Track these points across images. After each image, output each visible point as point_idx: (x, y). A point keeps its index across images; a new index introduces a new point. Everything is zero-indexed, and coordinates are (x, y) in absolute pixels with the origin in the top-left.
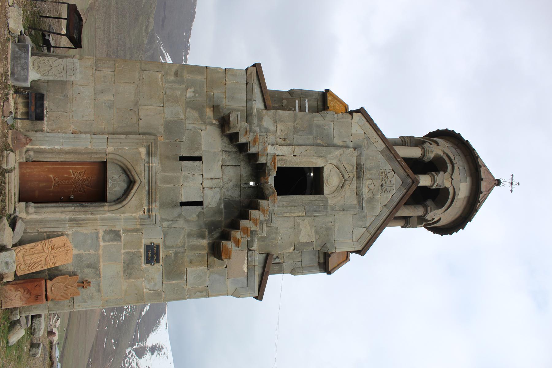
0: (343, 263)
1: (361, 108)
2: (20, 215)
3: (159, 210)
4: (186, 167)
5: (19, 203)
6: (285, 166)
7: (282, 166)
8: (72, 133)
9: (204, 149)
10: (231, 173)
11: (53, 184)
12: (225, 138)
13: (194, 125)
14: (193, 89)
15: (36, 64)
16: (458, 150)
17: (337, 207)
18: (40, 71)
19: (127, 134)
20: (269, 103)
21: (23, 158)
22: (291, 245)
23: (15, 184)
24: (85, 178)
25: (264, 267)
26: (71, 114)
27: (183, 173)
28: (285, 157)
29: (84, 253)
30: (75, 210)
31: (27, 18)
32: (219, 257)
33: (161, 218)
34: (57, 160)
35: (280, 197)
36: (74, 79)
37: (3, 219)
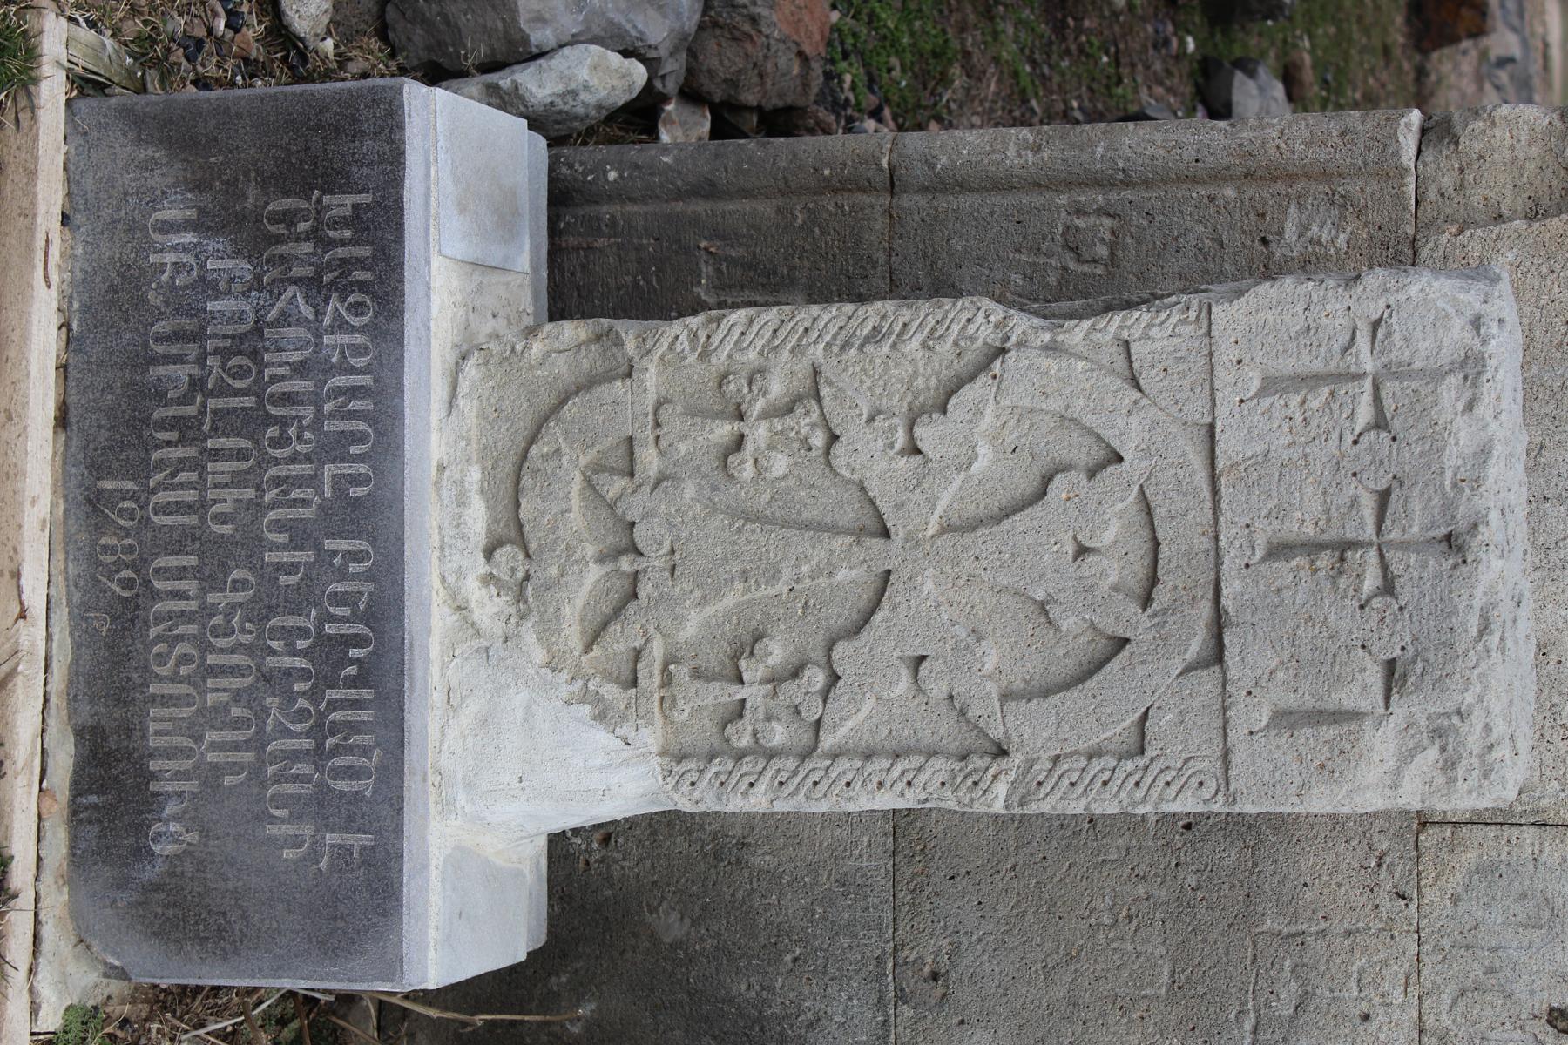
18: (657, 650)
36: (1410, 797)
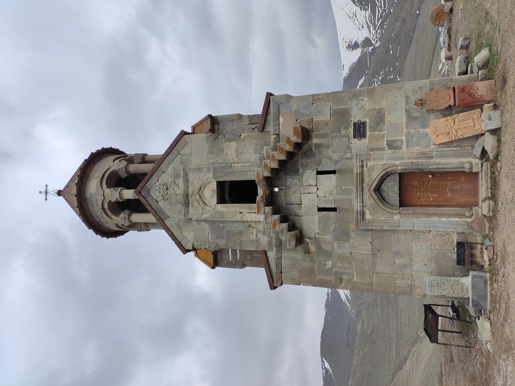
0: (198, 124)
1: (185, 254)
2: (478, 161)
3: (353, 167)
4: (331, 202)
5: (479, 171)
6: (249, 204)
7: (251, 204)
8: (431, 231)
9: (317, 218)
10: (294, 199)
11: (447, 187)
12: (299, 226)
13: (325, 237)
14: (327, 267)
15: (465, 291)
16: (98, 220)
17: (205, 171)
19: (382, 230)
20: (262, 256)
21: (475, 210)
22: (243, 139)
23: (482, 188)
24: (418, 194)
25: (265, 120)
26: (433, 248)
27: (333, 198)
28: (249, 211)
29: (420, 130)
30: (428, 165)
31: (474, 331)
32: (303, 128)
33: (352, 160)
34: (444, 208)
35: (253, 179)
36: (431, 277)
37: (493, 157)
